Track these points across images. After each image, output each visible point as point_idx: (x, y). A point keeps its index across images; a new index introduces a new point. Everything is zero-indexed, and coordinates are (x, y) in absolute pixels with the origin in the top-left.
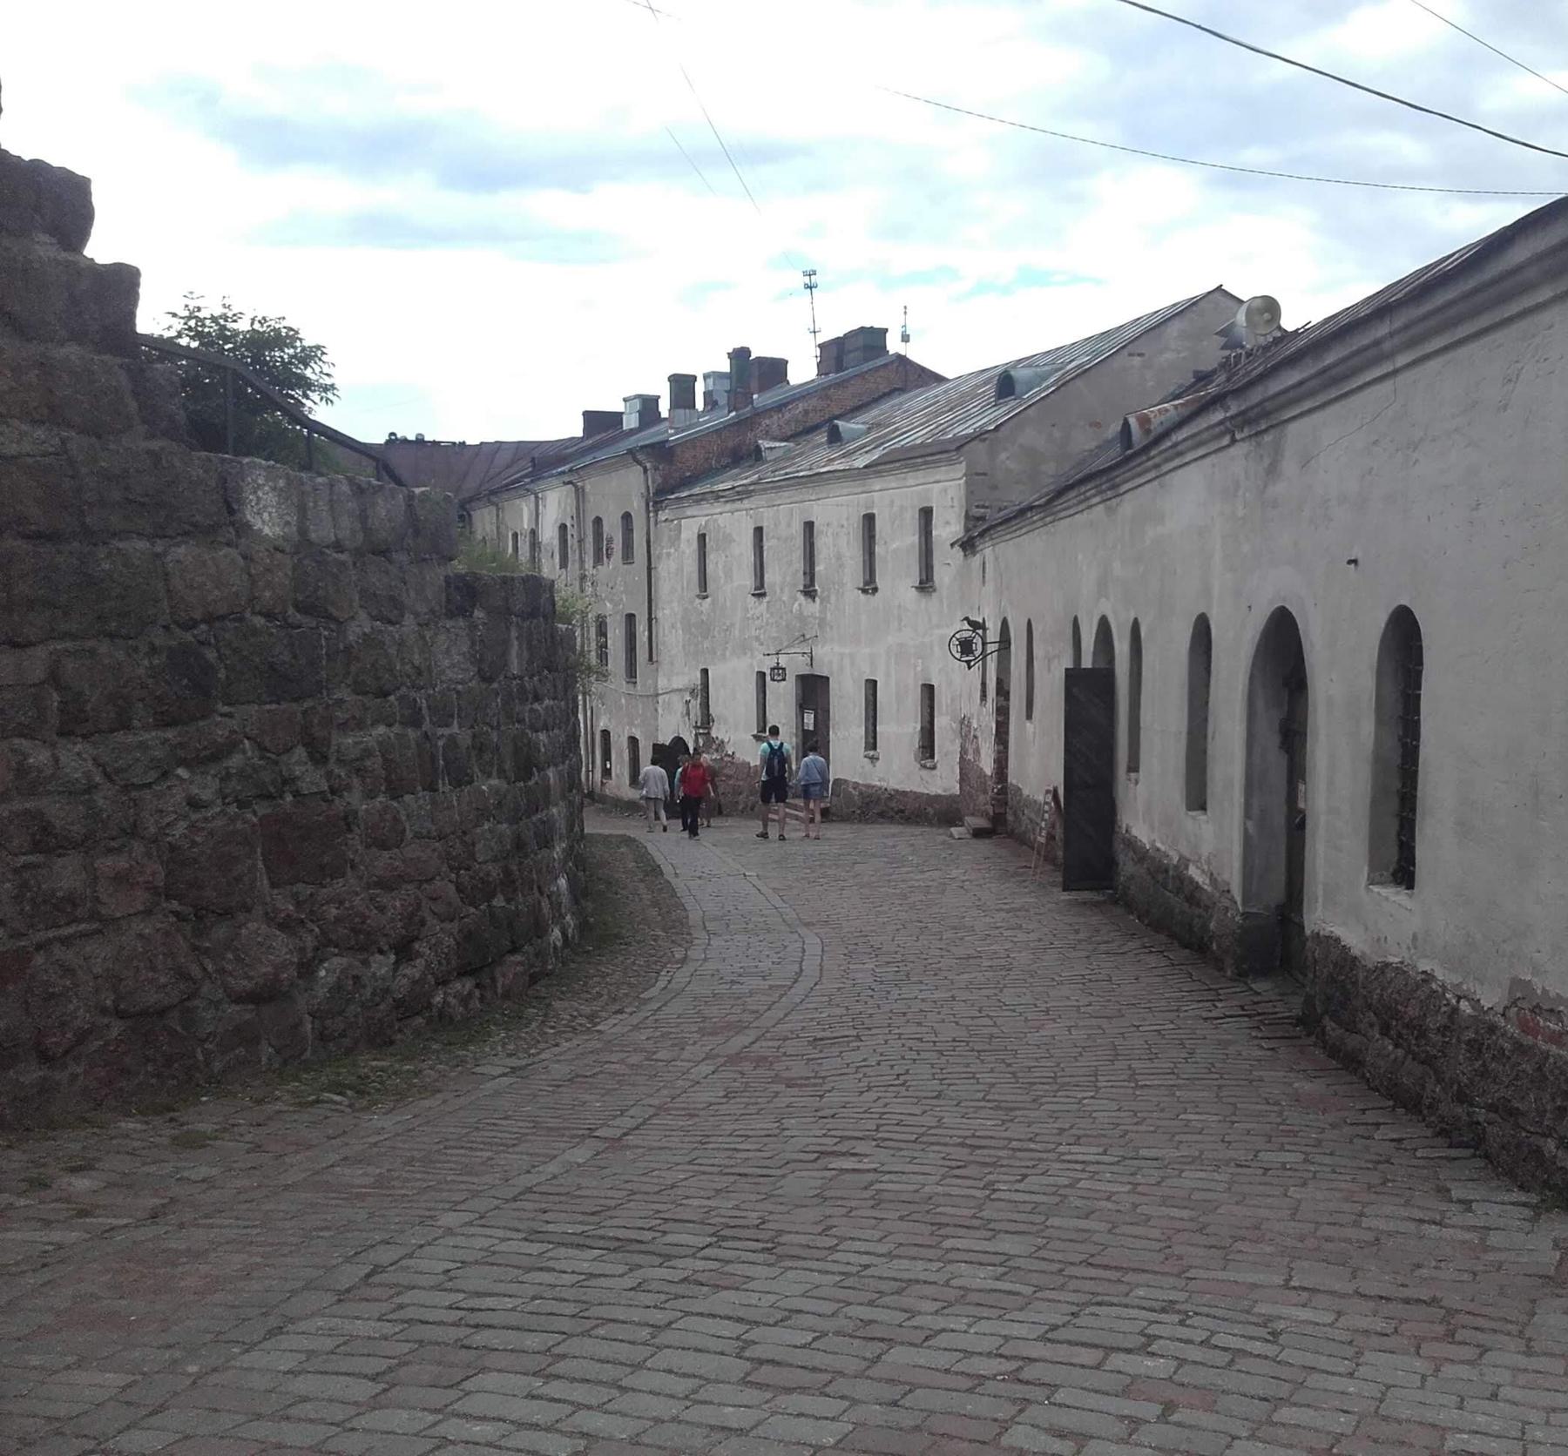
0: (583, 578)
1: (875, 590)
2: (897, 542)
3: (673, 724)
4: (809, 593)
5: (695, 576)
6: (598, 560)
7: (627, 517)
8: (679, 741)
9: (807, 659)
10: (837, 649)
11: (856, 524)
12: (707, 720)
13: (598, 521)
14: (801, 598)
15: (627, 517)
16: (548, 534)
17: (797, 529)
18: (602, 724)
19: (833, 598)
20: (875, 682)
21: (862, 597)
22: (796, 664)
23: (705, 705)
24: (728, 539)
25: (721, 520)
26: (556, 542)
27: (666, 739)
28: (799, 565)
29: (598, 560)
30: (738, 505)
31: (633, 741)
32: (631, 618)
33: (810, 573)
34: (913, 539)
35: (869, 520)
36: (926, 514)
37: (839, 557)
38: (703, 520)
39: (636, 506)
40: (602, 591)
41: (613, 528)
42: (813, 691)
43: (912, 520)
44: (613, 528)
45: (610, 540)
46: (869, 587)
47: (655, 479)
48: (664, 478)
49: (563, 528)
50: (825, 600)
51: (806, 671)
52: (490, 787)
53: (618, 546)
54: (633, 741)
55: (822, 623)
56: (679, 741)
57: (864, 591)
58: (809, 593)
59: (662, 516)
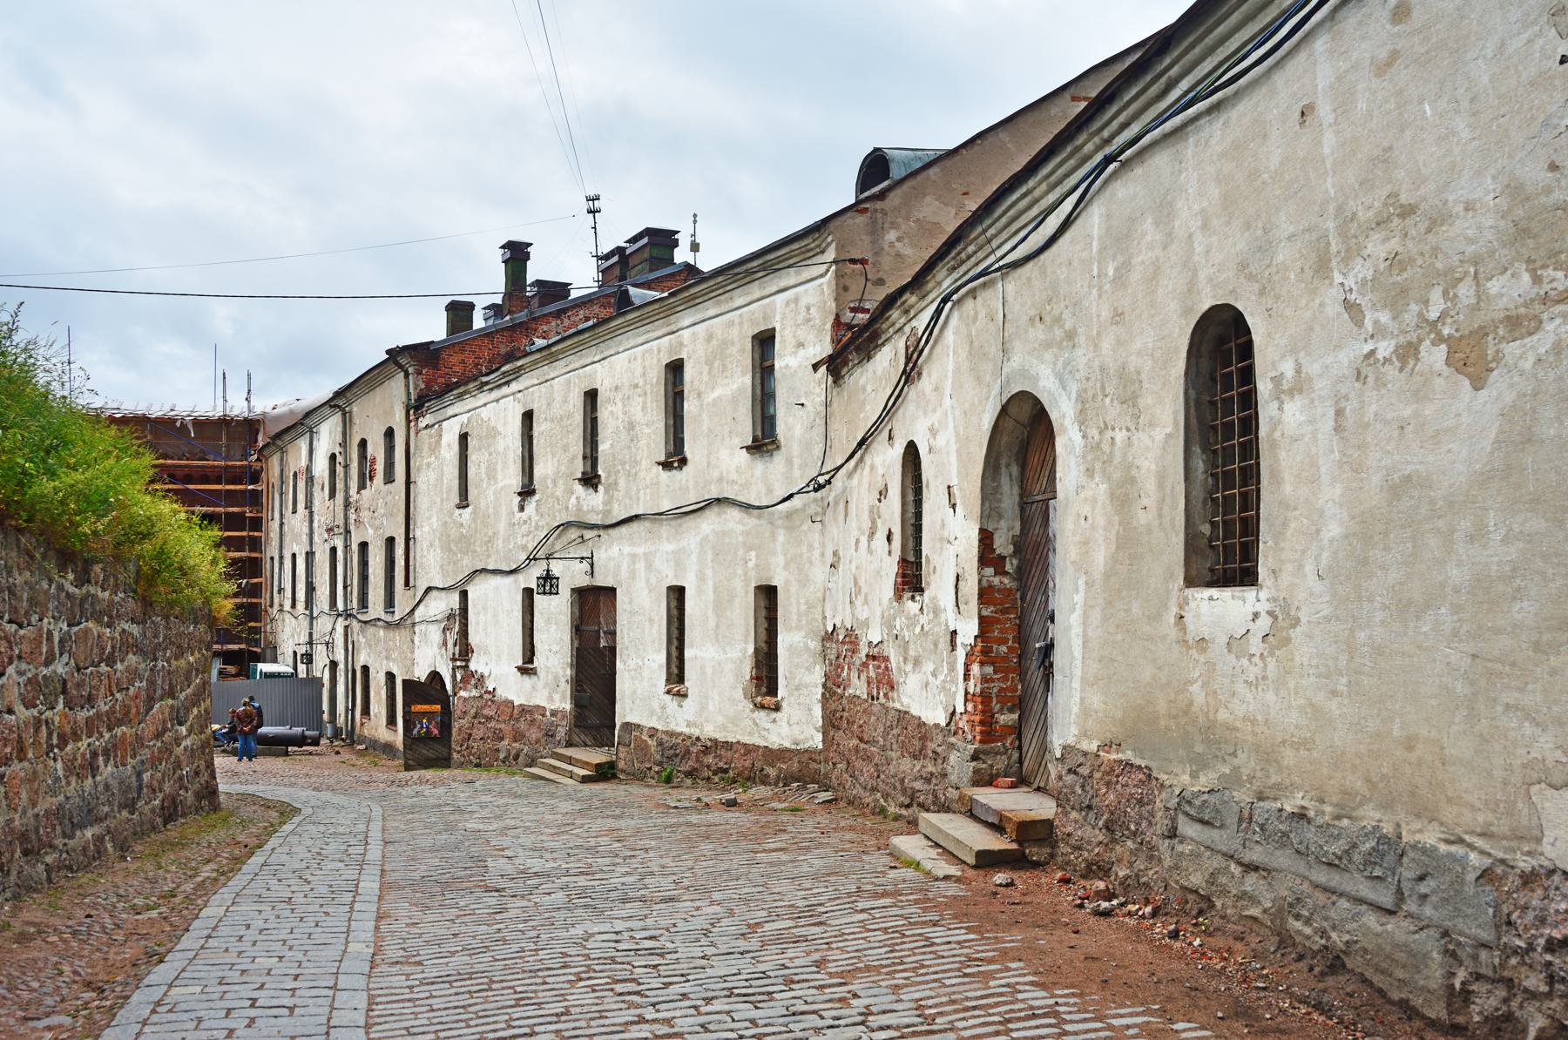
0: (347, 505)
1: (683, 461)
3: (427, 655)
6: (362, 486)
7: (390, 434)
8: (435, 676)
9: (585, 566)
10: (627, 550)
12: (465, 651)
13: (363, 444)
14: (579, 489)
15: (390, 434)
16: (321, 468)
17: (576, 402)
18: (362, 659)
19: (622, 482)
21: (664, 475)
22: (571, 574)
23: (464, 633)
24: (493, 433)
25: (485, 413)
26: (326, 474)
27: (421, 674)
28: (577, 448)
29: (362, 486)
30: (505, 390)
31: (390, 677)
32: (391, 541)
33: (591, 456)
37: (631, 426)
38: (464, 418)
39: (398, 420)
40: (365, 514)
41: (376, 450)
42: (594, 603)
44: (376, 450)
45: (373, 461)
47: (417, 384)
48: (428, 384)
49: (333, 457)
51: (584, 581)
53: (380, 467)
54: (390, 677)
56: (435, 676)
57: (666, 465)
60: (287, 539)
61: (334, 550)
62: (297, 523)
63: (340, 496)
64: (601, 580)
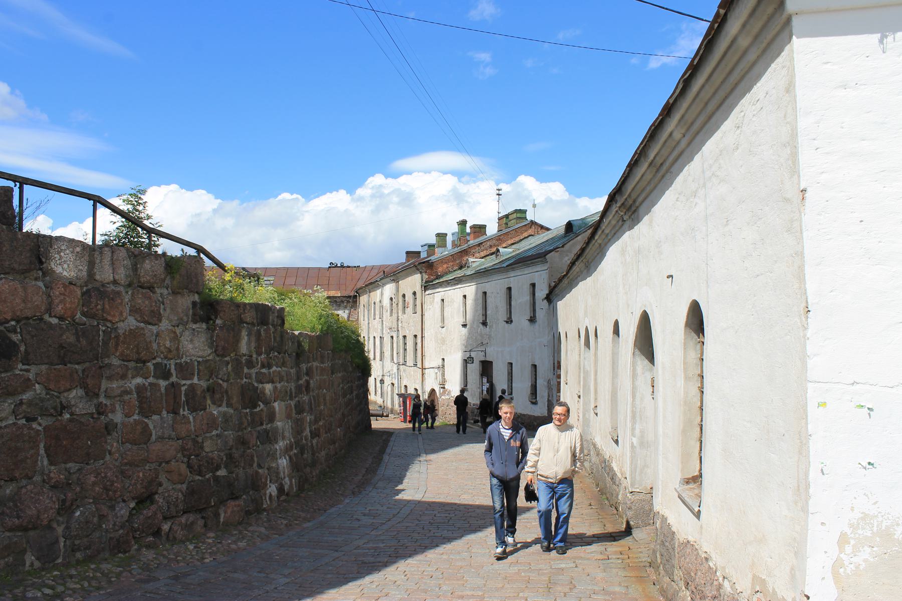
1: (512, 321)
2: (521, 299)
4: (484, 323)
5: (440, 317)
11: (504, 290)
13: (404, 296)
15: (414, 293)
16: (386, 302)
20: (511, 364)
21: (506, 325)
22: (478, 357)
23: (443, 375)
32: (415, 336)
33: (485, 315)
34: (527, 298)
35: (509, 289)
36: (533, 285)
37: (497, 307)
41: (409, 298)
43: (527, 289)
44: (409, 298)
46: (509, 321)
49: (391, 299)
50: (491, 327)
51: (483, 359)
52: (219, 412)
55: (490, 337)
57: (507, 322)
58: (484, 323)
59: (427, 292)
60: (371, 331)
61: (392, 337)
62: (376, 323)
63: (395, 315)
64: (488, 359)
